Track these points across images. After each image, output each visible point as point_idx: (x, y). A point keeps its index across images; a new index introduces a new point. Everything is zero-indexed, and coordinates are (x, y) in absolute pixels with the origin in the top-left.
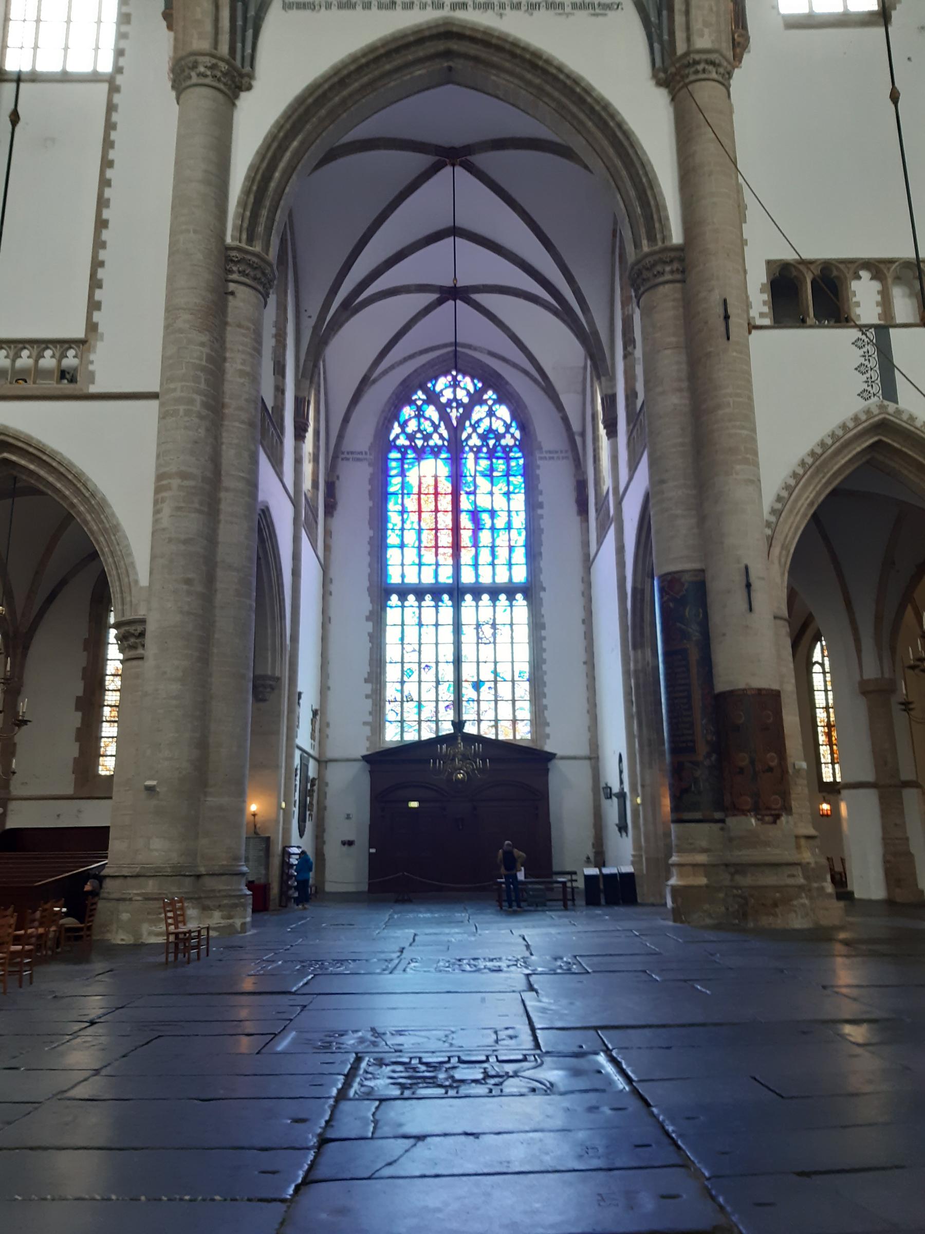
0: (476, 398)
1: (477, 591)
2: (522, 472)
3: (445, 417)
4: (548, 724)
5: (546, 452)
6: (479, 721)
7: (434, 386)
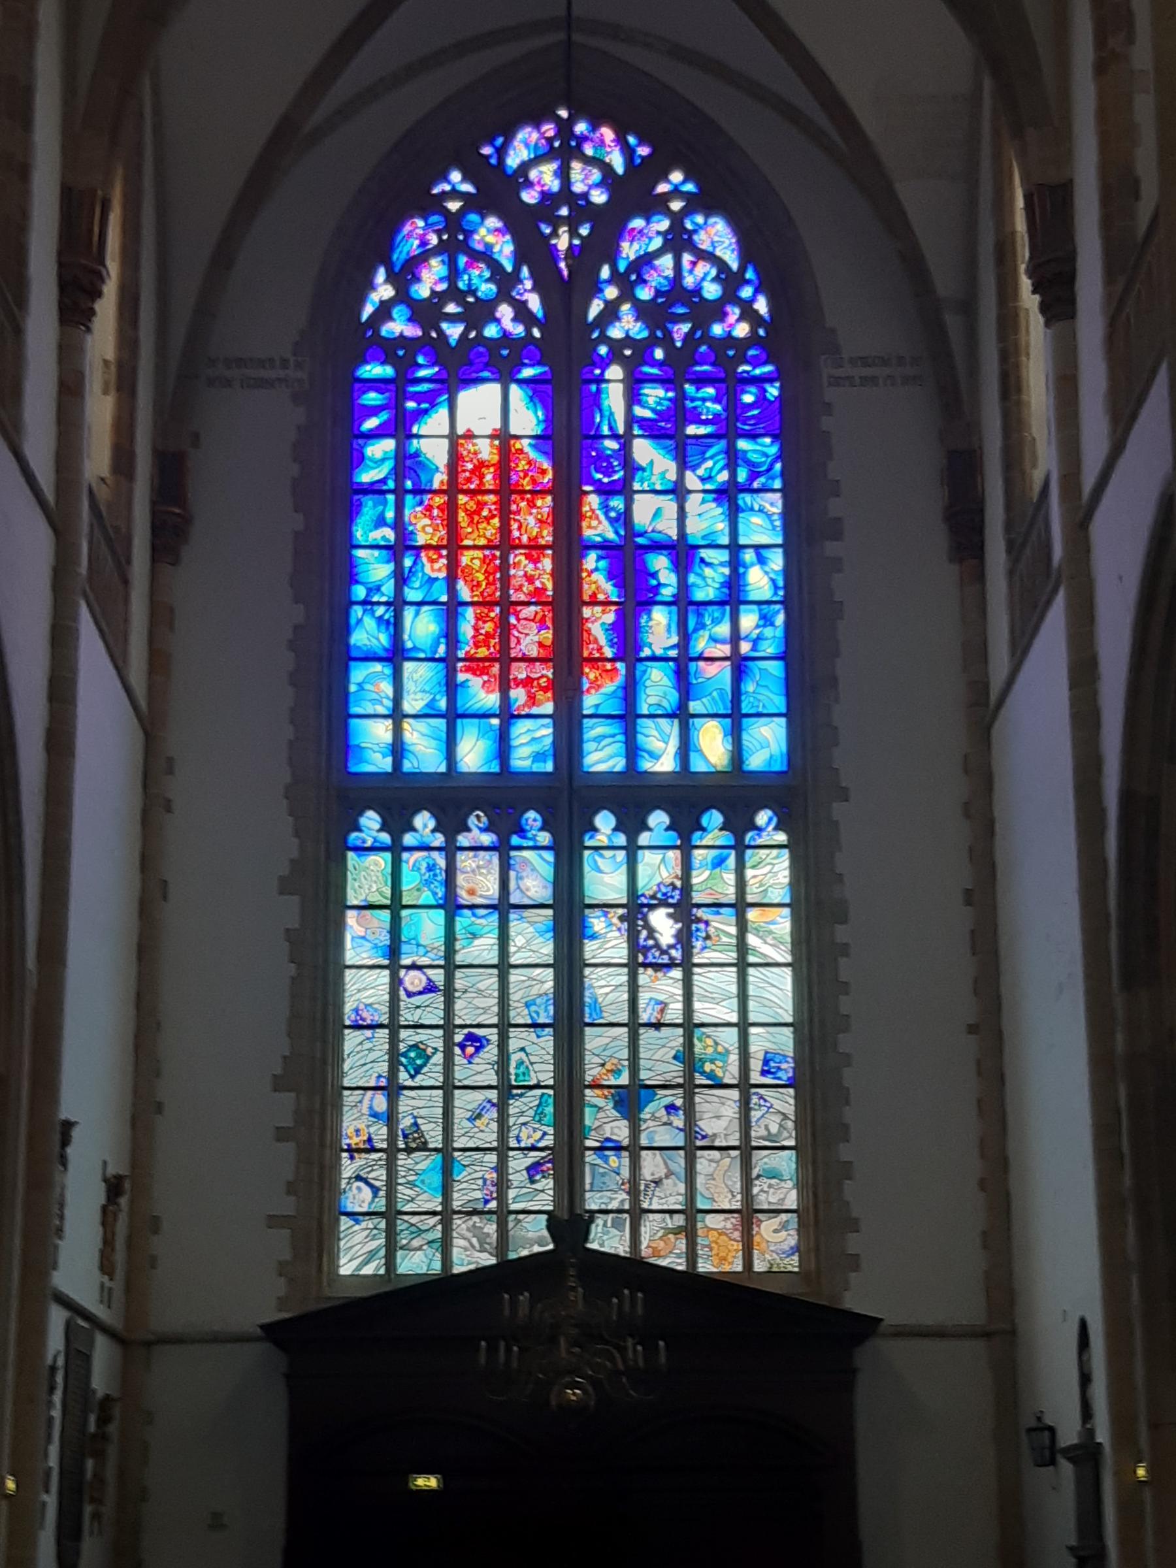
0: (633, 193)
1: (632, 797)
3: (532, 250)
5: (853, 361)
6: (637, 1213)
7: (501, 152)
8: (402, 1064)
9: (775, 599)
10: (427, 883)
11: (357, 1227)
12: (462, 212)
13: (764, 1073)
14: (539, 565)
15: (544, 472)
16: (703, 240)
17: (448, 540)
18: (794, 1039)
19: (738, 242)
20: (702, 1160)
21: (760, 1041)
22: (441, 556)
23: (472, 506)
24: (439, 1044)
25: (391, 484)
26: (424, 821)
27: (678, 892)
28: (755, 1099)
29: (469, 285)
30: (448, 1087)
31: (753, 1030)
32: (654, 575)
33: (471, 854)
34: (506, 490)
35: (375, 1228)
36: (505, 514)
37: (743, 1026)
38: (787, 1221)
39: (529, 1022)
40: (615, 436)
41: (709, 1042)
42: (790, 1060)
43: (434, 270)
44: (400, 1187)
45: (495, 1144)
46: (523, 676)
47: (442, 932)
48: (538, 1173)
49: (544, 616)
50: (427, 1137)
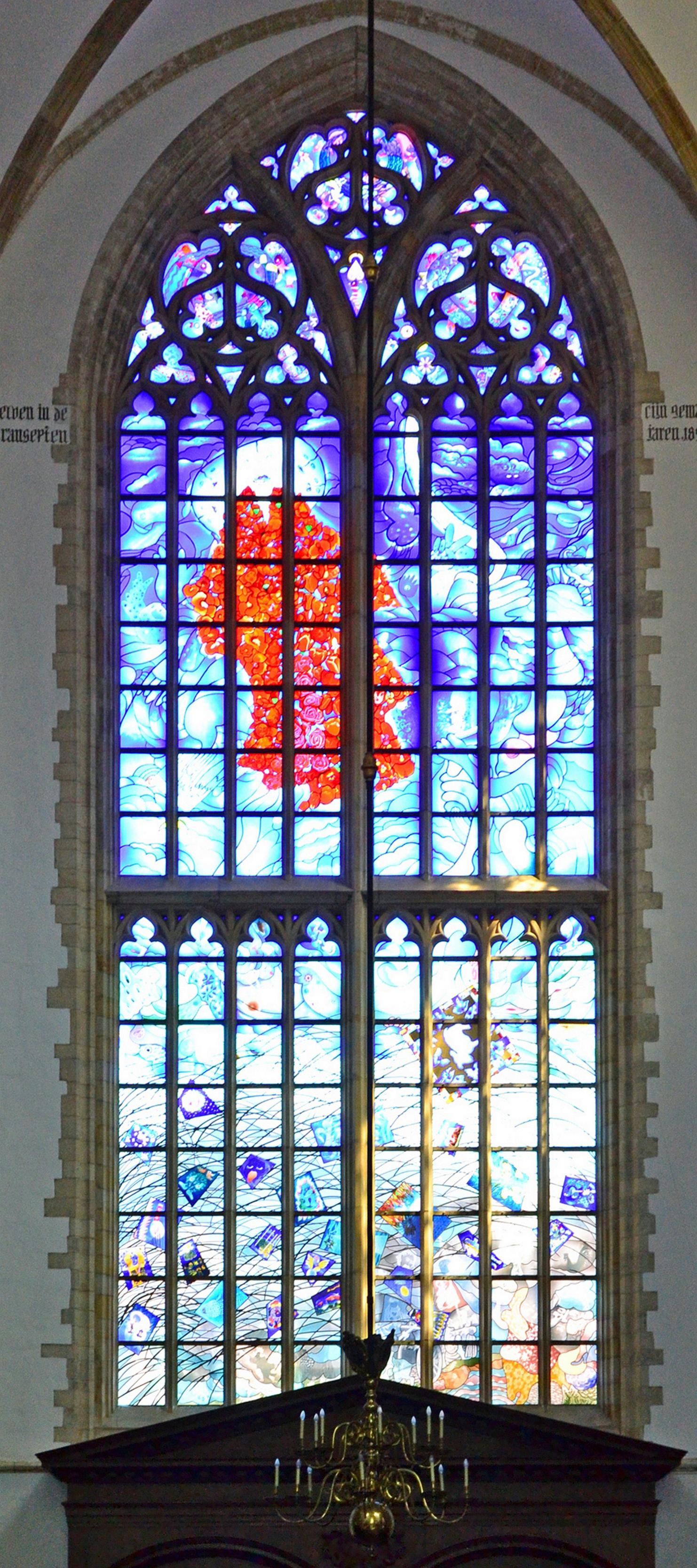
0: (432, 214)
1: (425, 905)
2: (587, 483)
3: (321, 283)
4: (657, 1357)
7: (285, 164)
8: (181, 1189)
9: (585, 683)
10: (205, 996)
11: (136, 1357)
12: (240, 236)
14: (326, 645)
15: (330, 539)
16: (511, 269)
17: (225, 616)
19: (549, 272)
21: (562, 1167)
22: (219, 635)
23: (252, 577)
24: (219, 1168)
25: (163, 554)
26: (202, 929)
27: (475, 1007)
28: (554, 1227)
29: (248, 323)
32: (452, 656)
33: (253, 964)
36: (288, 588)
37: (543, 1152)
38: (587, 1353)
39: (315, 1145)
40: (408, 498)
42: (593, 1187)
43: (208, 304)
44: (180, 1317)
45: (279, 1273)
46: (307, 769)
48: (324, 1303)
49: (332, 702)
50: (208, 1265)
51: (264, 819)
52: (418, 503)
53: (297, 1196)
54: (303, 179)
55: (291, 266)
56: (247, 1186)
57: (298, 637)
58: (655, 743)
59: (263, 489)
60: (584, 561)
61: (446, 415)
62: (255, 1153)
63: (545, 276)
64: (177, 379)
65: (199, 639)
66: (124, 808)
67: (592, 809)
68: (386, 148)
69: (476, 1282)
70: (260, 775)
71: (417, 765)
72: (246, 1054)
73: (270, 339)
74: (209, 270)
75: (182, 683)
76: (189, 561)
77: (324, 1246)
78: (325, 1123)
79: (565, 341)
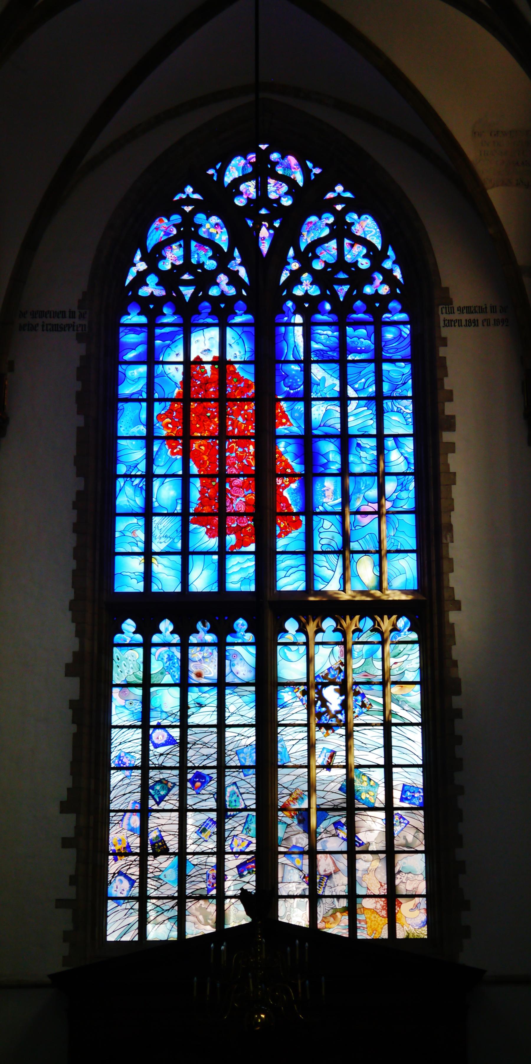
0: (310, 199)
7: (221, 173)
11: (119, 908)
13: (402, 800)
15: (248, 387)
16: (357, 230)
17: (183, 433)
18: (423, 776)
19: (381, 232)
20: (360, 861)
24: (176, 780)
25: (144, 395)
26: (166, 626)
27: (342, 674)
28: (396, 818)
29: (198, 262)
30: (183, 810)
31: (394, 770)
32: (325, 455)
33: (199, 648)
34: (223, 400)
35: (131, 908)
37: (388, 766)
39: (239, 764)
40: (297, 362)
41: (365, 778)
42: (421, 791)
45: (215, 850)
46: (234, 525)
47: (177, 702)
48: (245, 870)
50: (168, 845)
51: (206, 556)
52: (302, 365)
53: (227, 799)
54: (232, 181)
55: (224, 230)
56: (194, 792)
57: (228, 445)
58: (453, 506)
59: (207, 358)
60: (406, 398)
61: (320, 313)
62: (200, 771)
63: (379, 234)
64: (155, 294)
65: (167, 446)
66: (118, 549)
67: (415, 548)
68: (281, 164)
69: (346, 856)
70: (204, 529)
71: (304, 522)
72: (193, 706)
73: (212, 270)
74: (175, 232)
75: (156, 473)
76: (160, 400)
77: (245, 832)
78: (245, 750)
79: (391, 271)
